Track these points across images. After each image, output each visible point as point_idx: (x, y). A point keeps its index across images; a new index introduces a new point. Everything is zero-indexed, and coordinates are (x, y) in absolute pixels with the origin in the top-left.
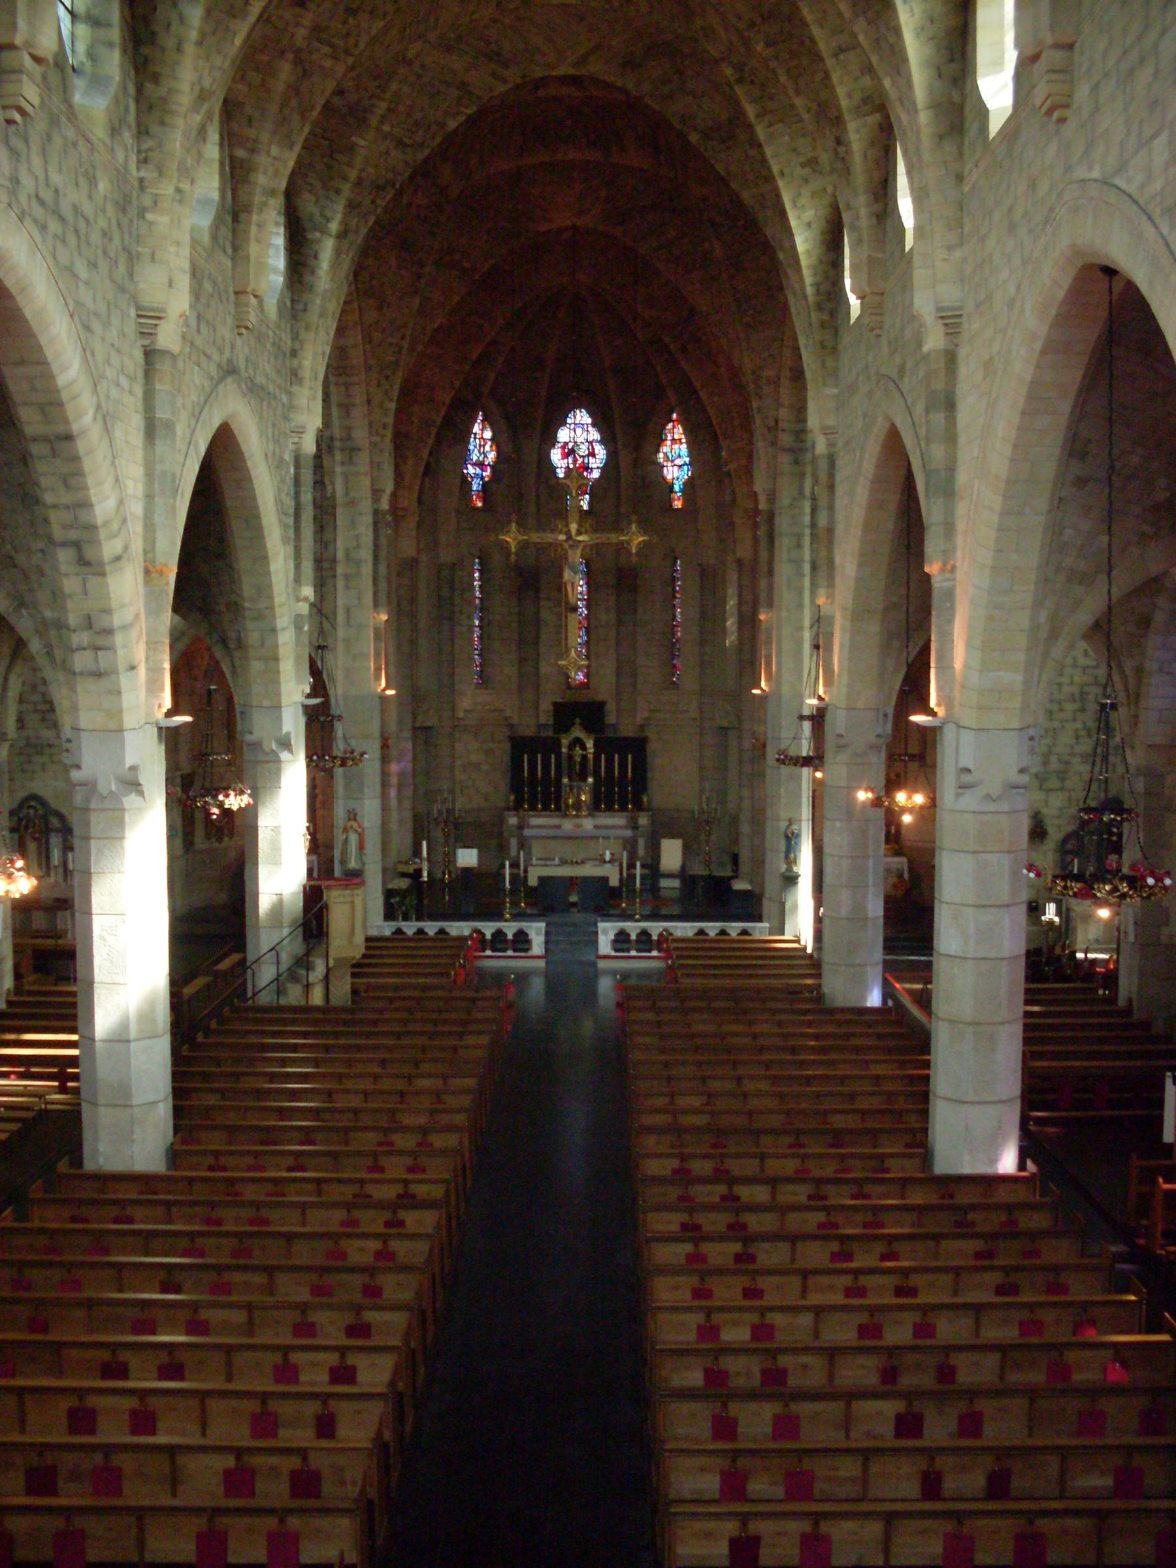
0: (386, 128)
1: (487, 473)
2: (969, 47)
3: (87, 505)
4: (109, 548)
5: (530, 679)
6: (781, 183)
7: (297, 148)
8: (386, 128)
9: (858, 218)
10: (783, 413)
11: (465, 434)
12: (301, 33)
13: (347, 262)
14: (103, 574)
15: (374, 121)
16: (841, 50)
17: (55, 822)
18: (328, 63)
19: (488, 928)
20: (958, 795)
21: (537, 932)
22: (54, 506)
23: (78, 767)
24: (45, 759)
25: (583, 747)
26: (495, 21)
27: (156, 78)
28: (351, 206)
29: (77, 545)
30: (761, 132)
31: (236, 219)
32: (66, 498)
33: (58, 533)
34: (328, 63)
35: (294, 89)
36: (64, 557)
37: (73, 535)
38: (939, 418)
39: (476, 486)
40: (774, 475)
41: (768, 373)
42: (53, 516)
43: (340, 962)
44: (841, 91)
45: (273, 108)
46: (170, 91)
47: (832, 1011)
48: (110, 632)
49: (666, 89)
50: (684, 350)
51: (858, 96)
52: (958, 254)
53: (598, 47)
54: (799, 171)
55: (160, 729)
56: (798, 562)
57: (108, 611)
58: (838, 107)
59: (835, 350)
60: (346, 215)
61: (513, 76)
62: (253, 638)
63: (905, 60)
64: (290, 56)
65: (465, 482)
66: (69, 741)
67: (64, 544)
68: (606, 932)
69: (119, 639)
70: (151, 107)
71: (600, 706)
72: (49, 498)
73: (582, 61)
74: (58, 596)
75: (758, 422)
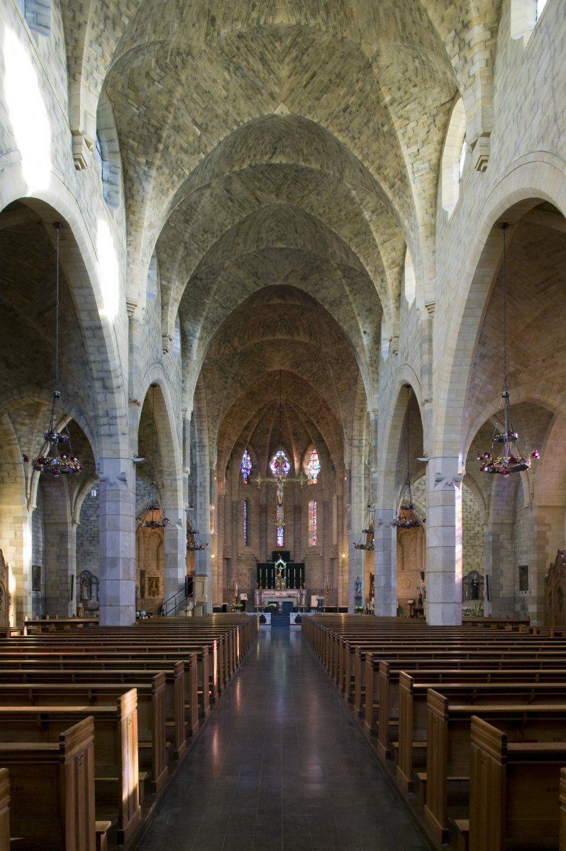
1: (249, 473)
6: (358, 318)
11: (240, 457)
12: (187, 235)
16: (385, 242)
26: (256, 257)
27: (134, 213)
28: (204, 328)
30: (351, 298)
34: (196, 252)
35: (184, 259)
44: (384, 259)
51: (390, 260)
70: (131, 225)
73: (286, 278)
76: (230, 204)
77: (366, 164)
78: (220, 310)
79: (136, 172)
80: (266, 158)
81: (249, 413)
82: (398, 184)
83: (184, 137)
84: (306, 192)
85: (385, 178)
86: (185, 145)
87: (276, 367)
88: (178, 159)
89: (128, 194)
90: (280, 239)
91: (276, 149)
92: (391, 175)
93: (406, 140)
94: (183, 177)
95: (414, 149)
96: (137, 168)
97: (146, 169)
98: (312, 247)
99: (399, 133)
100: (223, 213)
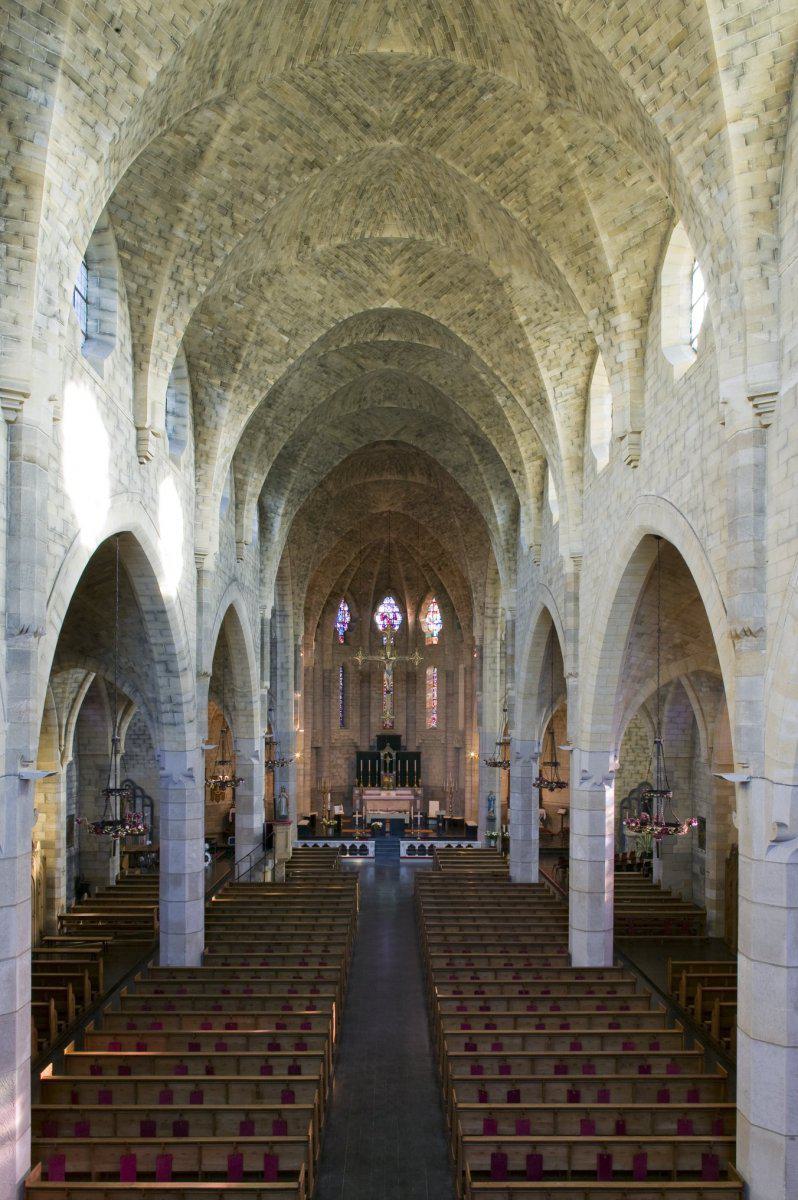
0: (305, 464)
1: (346, 627)
2: (586, 431)
3: (171, 644)
4: (181, 665)
5: (365, 724)
6: (490, 492)
7: (266, 475)
8: (305, 464)
9: (529, 509)
10: (488, 600)
11: (335, 609)
13: (286, 528)
14: (178, 677)
15: (300, 462)
16: (523, 430)
17: (139, 792)
18: (281, 434)
19: (348, 844)
20: (581, 783)
21: (371, 845)
22: (155, 644)
23: (163, 769)
24: (135, 762)
25: (391, 757)
27: (204, 442)
28: (289, 501)
29: (165, 663)
30: (481, 468)
31: (237, 507)
32: (161, 640)
33: (156, 656)
34: (281, 434)
36: (159, 668)
37: (163, 658)
38: (571, 605)
39: (341, 633)
40: (483, 629)
41: (481, 581)
42: (154, 648)
43: (280, 861)
44: (522, 449)
45: (255, 455)
46: (211, 448)
47: (515, 885)
48: (180, 704)
49: (436, 448)
50: (440, 569)
51: (530, 452)
52: (581, 527)
53: (406, 427)
54: (500, 487)
55: (203, 750)
56: (494, 670)
57: (180, 695)
58: (521, 457)
59: (515, 571)
60: (286, 506)
61: (365, 441)
62: (241, 706)
63: (556, 437)
64: (263, 431)
65: (336, 631)
66: (159, 756)
67: (159, 662)
68: (404, 845)
69: (185, 707)
71: (398, 738)
72: (153, 640)
73: (398, 433)
74: (154, 687)
75: (476, 604)
76: (325, 376)
77: (497, 373)
78: (310, 477)
79: (207, 394)
80: (371, 336)
81: (347, 557)
82: (537, 404)
83: (269, 348)
84: (422, 361)
85: (521, 394)
86: (270, 356)
87: (384, 508)
88: (260, 373)
89: (198, 420)
90: (389, 398)
91: (384, 327)
92: (528, 392)
93: (546, 362)
94: (267, 387)
95: (556, 372)
96: (209, 389)
97: (221, 391)
98: (431, 409)
99: (537, 355)
100: (316, 387)
